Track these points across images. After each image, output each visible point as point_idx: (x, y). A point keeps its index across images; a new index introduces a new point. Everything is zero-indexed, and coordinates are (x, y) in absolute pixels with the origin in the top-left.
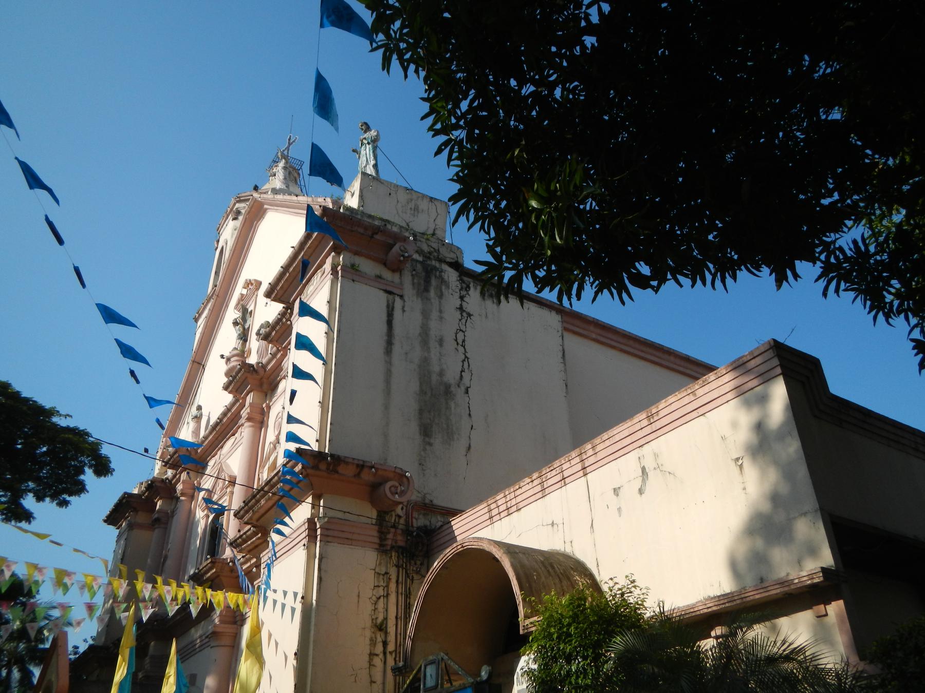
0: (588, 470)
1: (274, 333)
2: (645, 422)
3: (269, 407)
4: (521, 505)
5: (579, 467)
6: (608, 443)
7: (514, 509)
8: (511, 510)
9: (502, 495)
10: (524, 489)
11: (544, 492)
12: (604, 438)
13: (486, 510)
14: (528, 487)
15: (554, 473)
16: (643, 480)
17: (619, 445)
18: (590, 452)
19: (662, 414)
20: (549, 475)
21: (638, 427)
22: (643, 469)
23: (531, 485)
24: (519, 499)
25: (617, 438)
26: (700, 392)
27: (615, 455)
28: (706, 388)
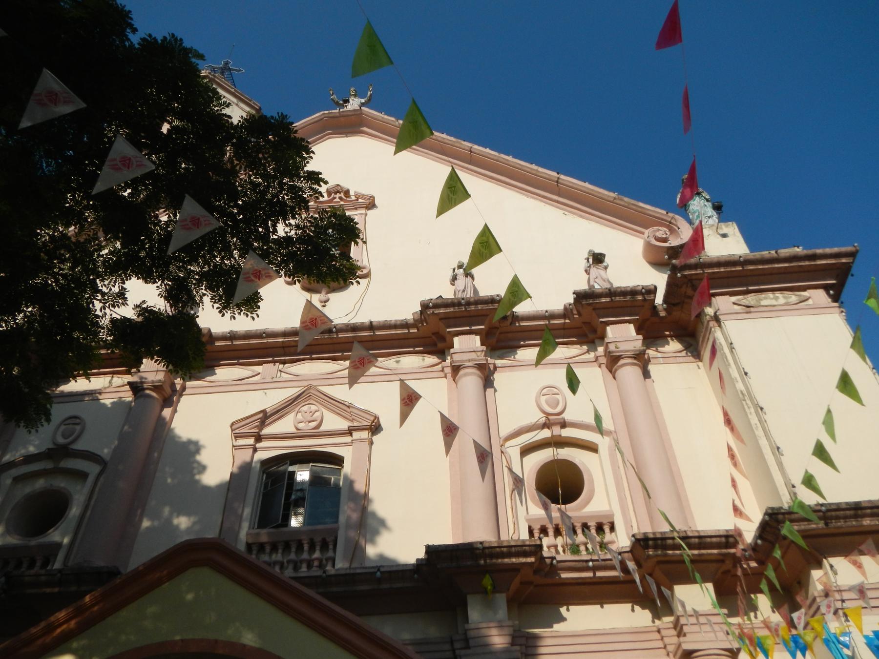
1: (603, 300)
3: (495, 368)
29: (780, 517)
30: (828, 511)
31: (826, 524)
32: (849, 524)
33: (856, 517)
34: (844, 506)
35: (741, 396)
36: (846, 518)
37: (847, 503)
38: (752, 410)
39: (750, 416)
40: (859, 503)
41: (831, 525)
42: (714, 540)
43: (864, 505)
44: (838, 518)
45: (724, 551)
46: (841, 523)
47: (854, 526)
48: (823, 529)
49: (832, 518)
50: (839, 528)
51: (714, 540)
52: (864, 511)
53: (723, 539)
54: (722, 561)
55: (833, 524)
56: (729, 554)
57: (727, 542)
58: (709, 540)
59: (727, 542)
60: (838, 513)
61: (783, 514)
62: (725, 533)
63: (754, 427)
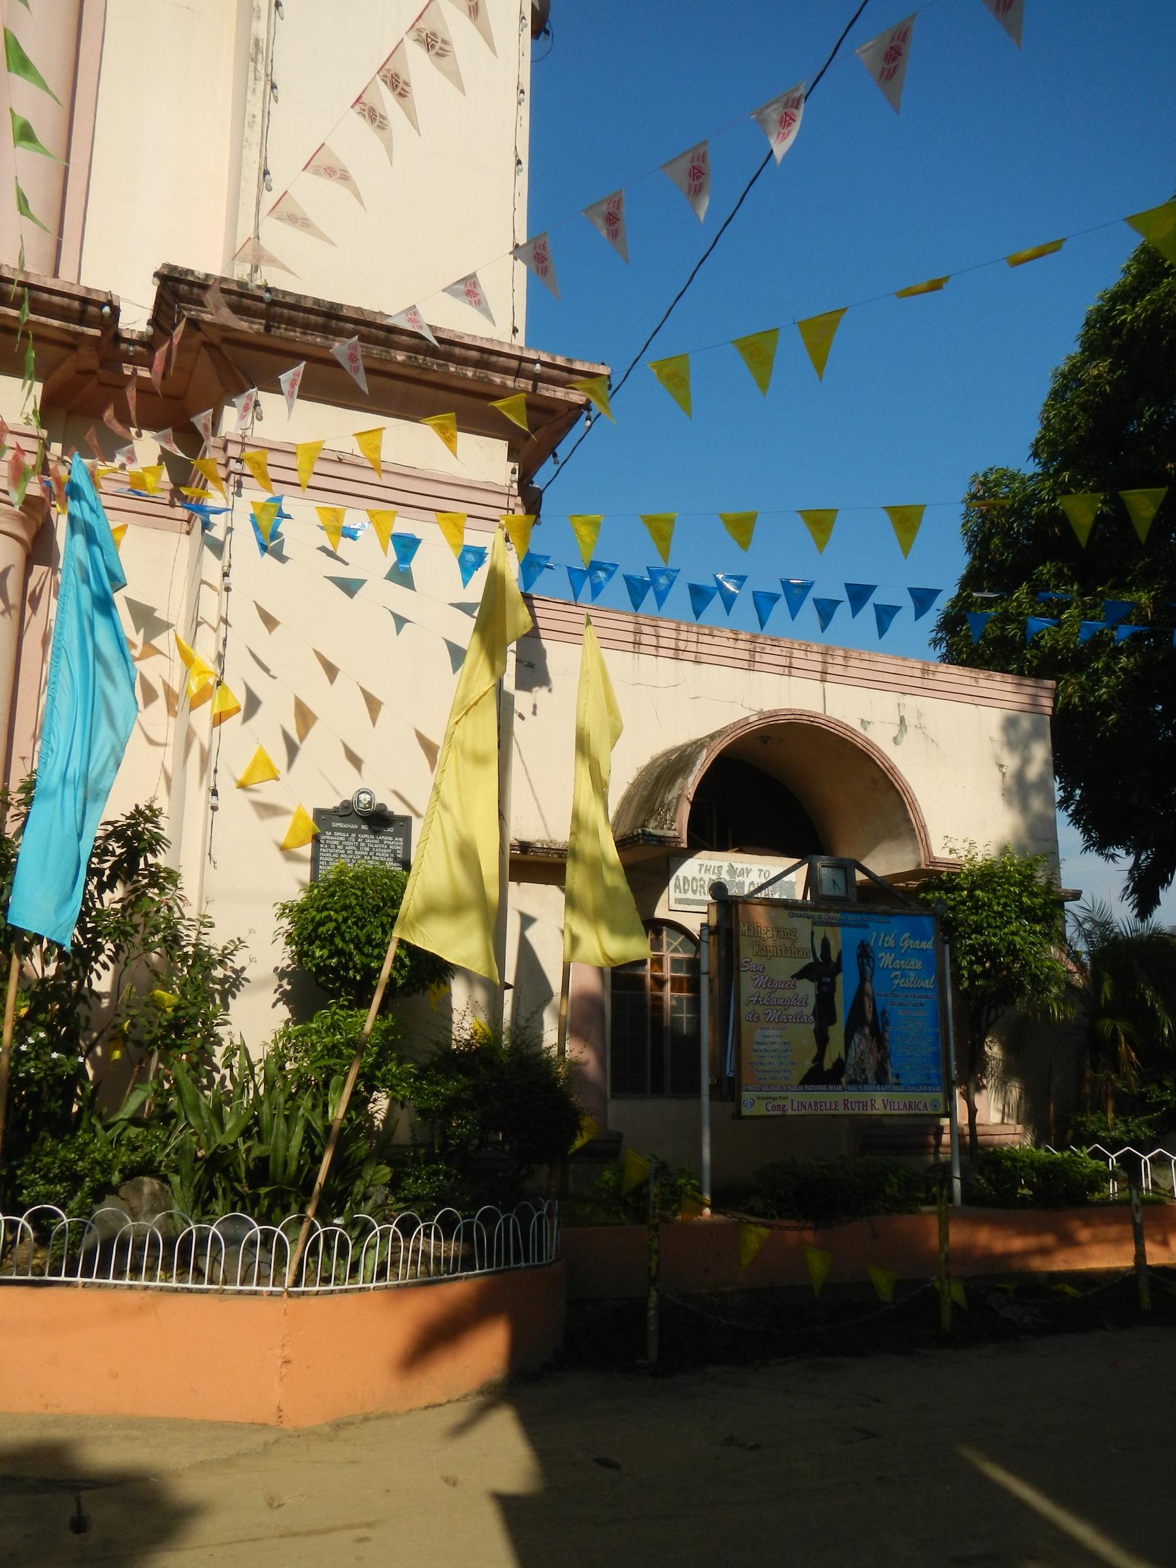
0: (829, 677)
2: (918, 673)
4: (704, 658)
5: (819, 667)
6: (865, 665)
7: (692, 656)
8: (682, 655)
9: (673, 626)
10: (716, 641)
11: (751, 664)
12: (863, 656)
13: (631, 627)
14: (724, 642)
15: (777, 650)
16: (900, 730)
17: (879, 677)
18: (840, 660)
19: (939, 676)
20: (768, 649)
21: (908, 672)
22: (902, 719)
23: (731, 643)
24: (703, 648)
25: (880, 667)
26: (983, 683)
27: (870, 683)
28: (989, 684)
29: (183, 288)
30: (273, 303)
31: (268, 328)
32: (309, 338)
33: (325, 330)
34: (309, 304)
35: (252, 49)
36: (306, 327)
37: (317, 301)
38: (260, 86)
39: (249, 96)
40: (341, 306)
41: (274, 331)
42: (56, 299)
43: (345, 312)
44: (291, 323)
45: (73, 327)
46: (296, 334)
47: (316, 345)
48: (258, 333)
49: (280, 319)
50: (288, 340)
51: (56, 299)
52: (342, 324)
53: (76, 304)
54: (73, 347)
55: (281, 331)
56: (82, 334)
57: (83, 312)
58: (45, 296)
59: (83, 312)
60: (294, 313)
61: (191, 284)
62: (82, 294)
63: (248, 118)
